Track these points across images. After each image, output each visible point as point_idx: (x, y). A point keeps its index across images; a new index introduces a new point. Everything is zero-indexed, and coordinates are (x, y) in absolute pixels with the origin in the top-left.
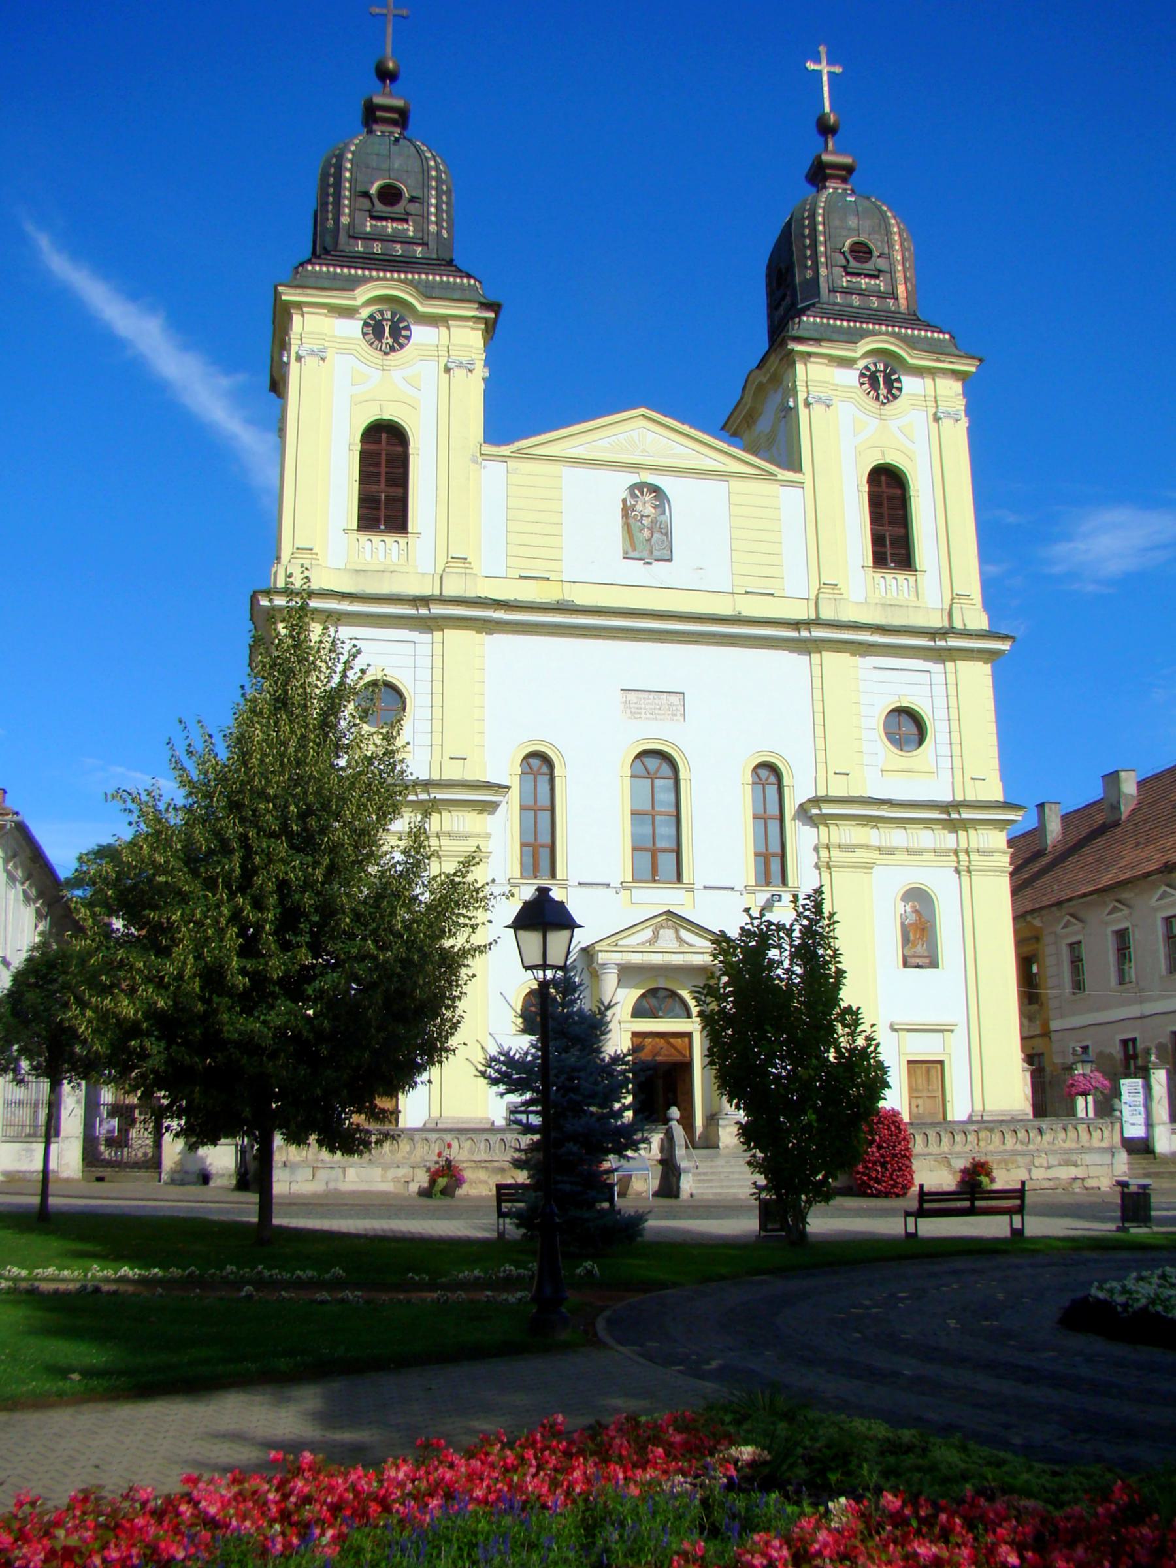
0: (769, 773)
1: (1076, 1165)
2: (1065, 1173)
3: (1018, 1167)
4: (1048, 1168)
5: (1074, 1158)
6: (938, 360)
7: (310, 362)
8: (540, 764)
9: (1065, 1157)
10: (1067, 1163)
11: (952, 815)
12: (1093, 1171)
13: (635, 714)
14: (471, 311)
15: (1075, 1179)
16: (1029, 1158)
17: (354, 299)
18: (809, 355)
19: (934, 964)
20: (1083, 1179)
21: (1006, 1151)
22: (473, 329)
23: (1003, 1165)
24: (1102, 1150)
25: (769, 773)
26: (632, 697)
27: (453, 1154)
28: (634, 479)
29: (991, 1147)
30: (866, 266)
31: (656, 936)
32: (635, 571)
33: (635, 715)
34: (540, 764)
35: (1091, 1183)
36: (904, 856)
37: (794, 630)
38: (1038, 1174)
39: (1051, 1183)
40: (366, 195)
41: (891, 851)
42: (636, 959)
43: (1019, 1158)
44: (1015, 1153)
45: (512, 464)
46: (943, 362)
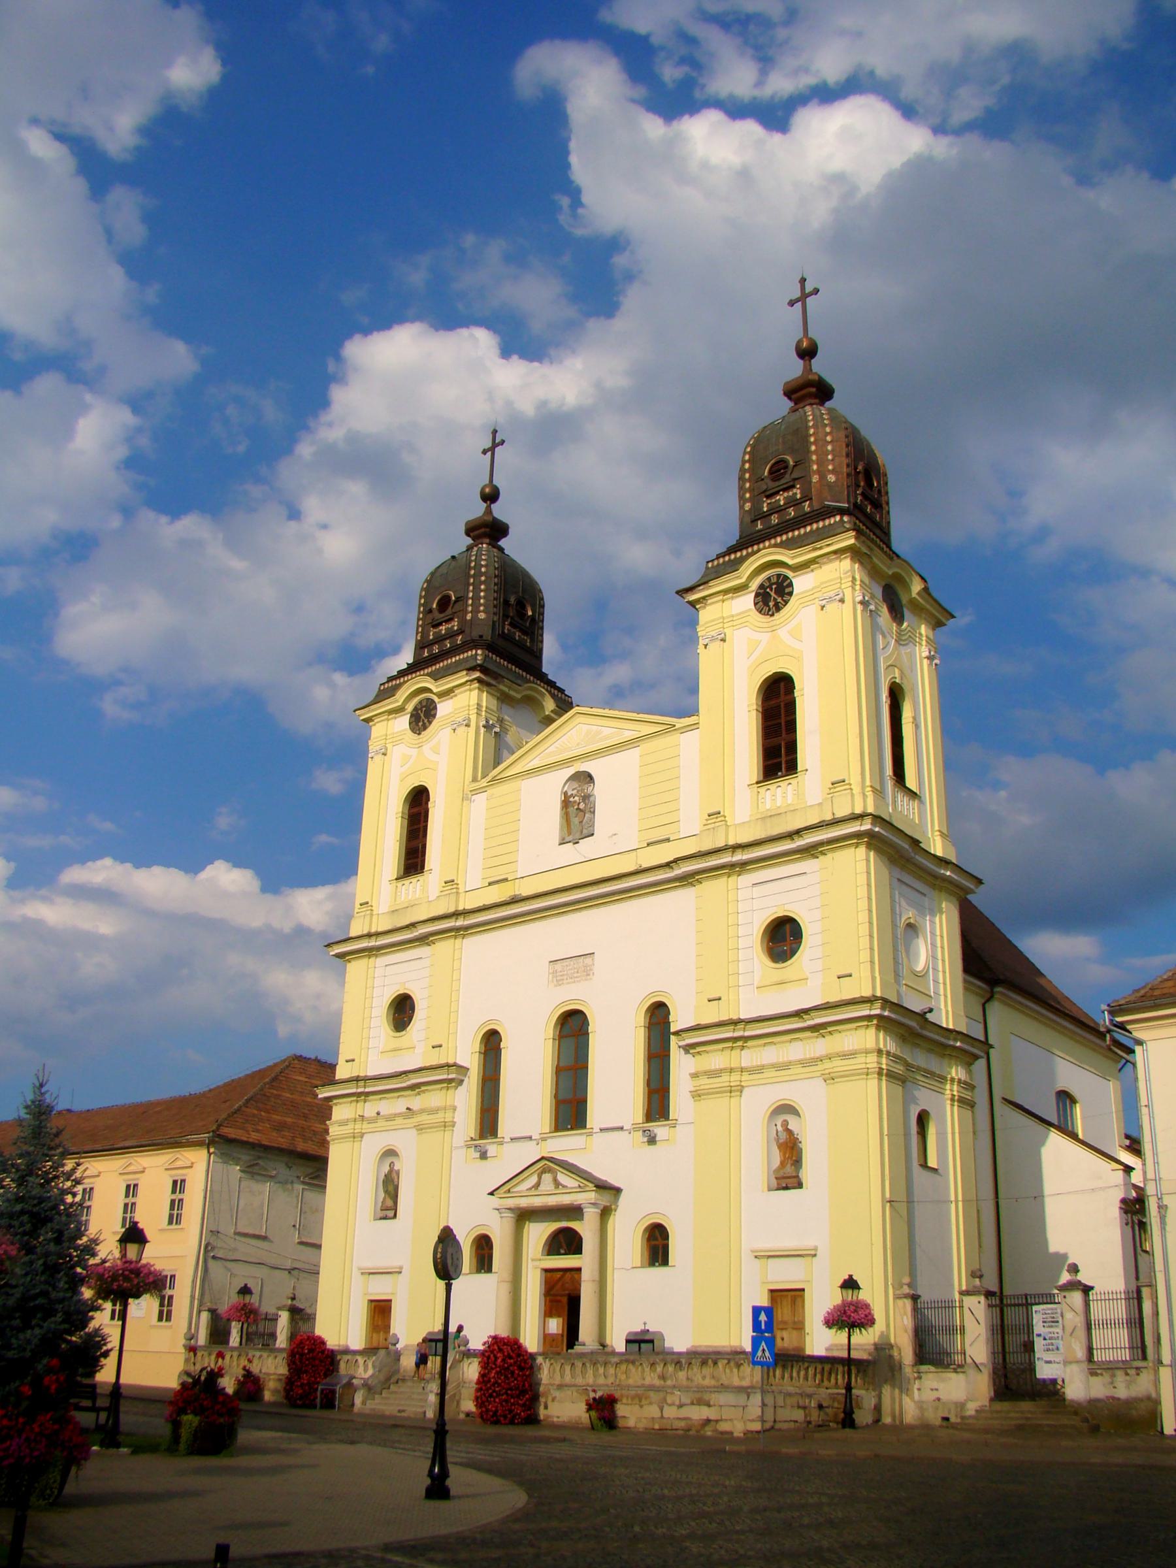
0: (658, 1013)
1: (709, 1406)
2: (698, 1413)
3: (651, 1403)
4: (681, 1406)
5: (706, 1397)
6: (815, 549)
7: (378, 758)
8: (492, 1042)
9: (698, 1395)
10: (700, 1402)
11: (810, 1021)
12: (727, 1413)
13: (558, 979)
14: (462, 677)
15: (708, 1421)
16: (662, 1395)
17: (397, 701)
18: (704, 598)
19: (800, 1185)
20: (717, 1421)
21: (643, 1386)
22: (470, 690)
23: (637, 1401)
24: (740, 1390)
25: (658, 1013)
26: (558, 966)
27: (255, 1368)
28: (570, 771)
29: (631, 1381)
30: (783, 481)
31: (537, 1185)
32: (570, 853)
33: (559, 983)
34: (492, 1042)
35: (724, 1427)
36: (771, 1073)
37: (667, 870)
38: (670, 1412)
39: (682, 1424)
40: (430, 611)
41: (759, 1069)
42: (524, 1203)
43: (652, 1394)
44: (652, 1388)
45: (490, 791)
46: (821, 548)
